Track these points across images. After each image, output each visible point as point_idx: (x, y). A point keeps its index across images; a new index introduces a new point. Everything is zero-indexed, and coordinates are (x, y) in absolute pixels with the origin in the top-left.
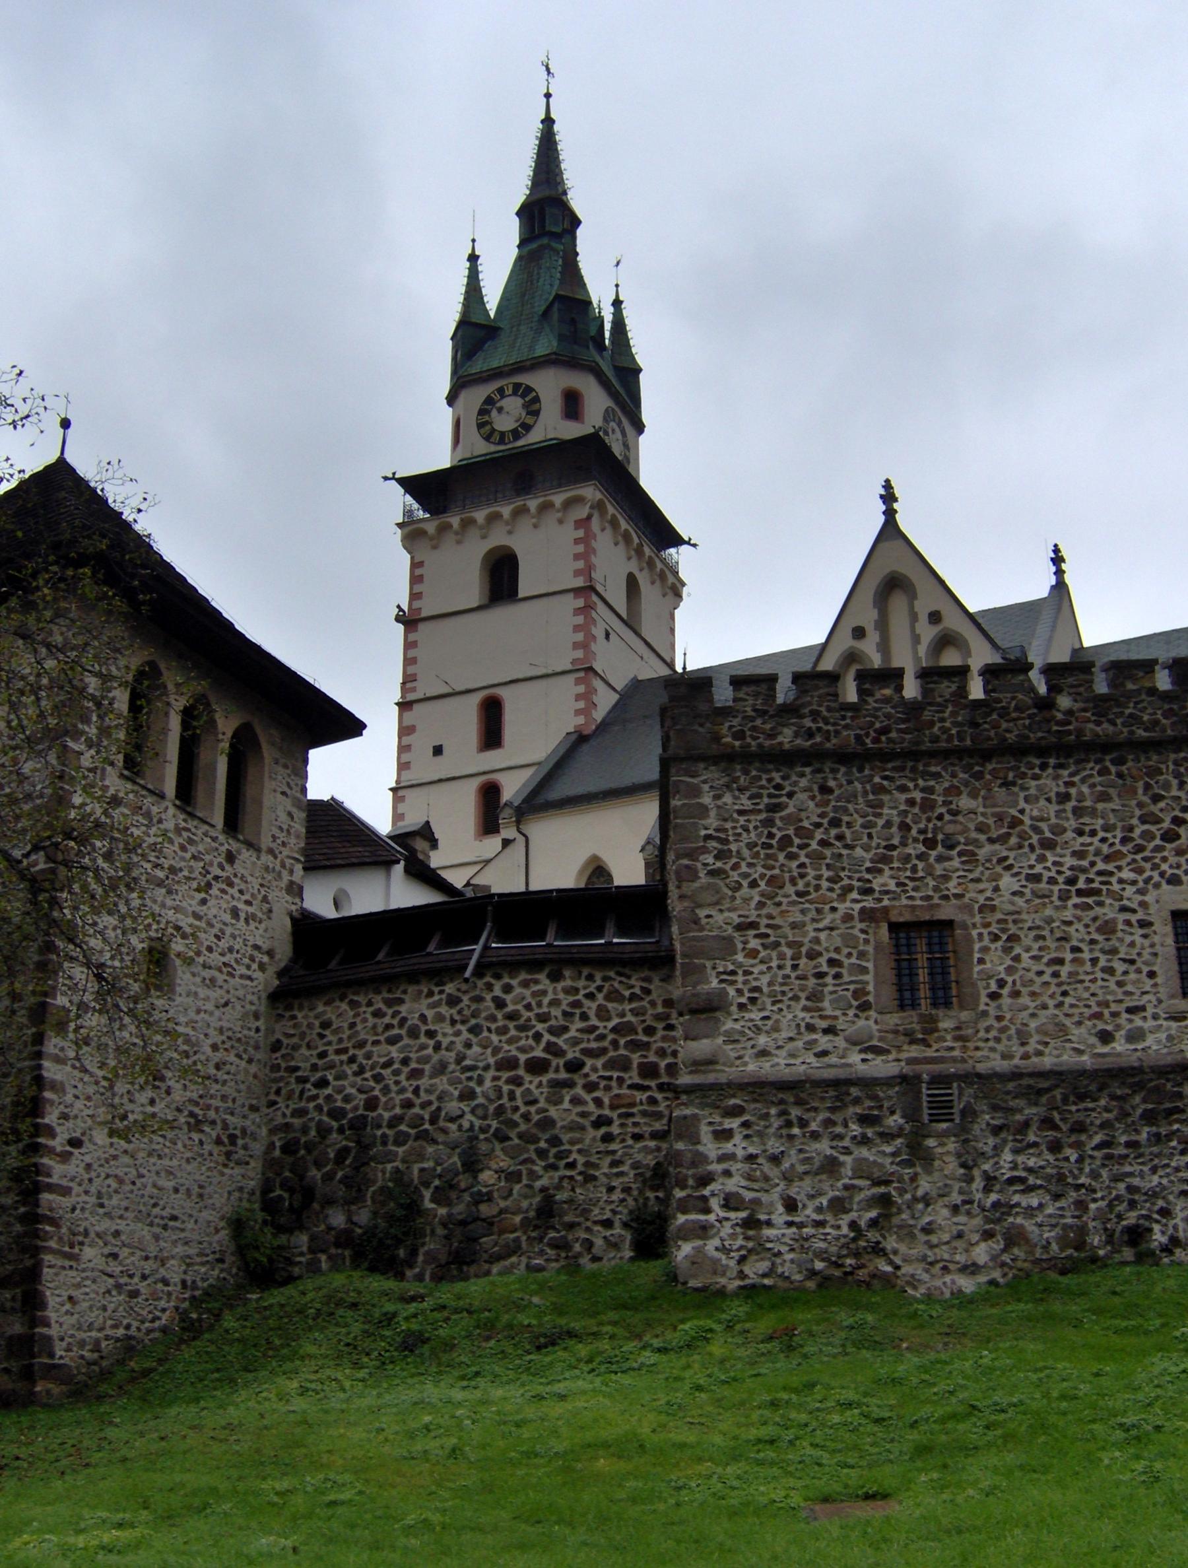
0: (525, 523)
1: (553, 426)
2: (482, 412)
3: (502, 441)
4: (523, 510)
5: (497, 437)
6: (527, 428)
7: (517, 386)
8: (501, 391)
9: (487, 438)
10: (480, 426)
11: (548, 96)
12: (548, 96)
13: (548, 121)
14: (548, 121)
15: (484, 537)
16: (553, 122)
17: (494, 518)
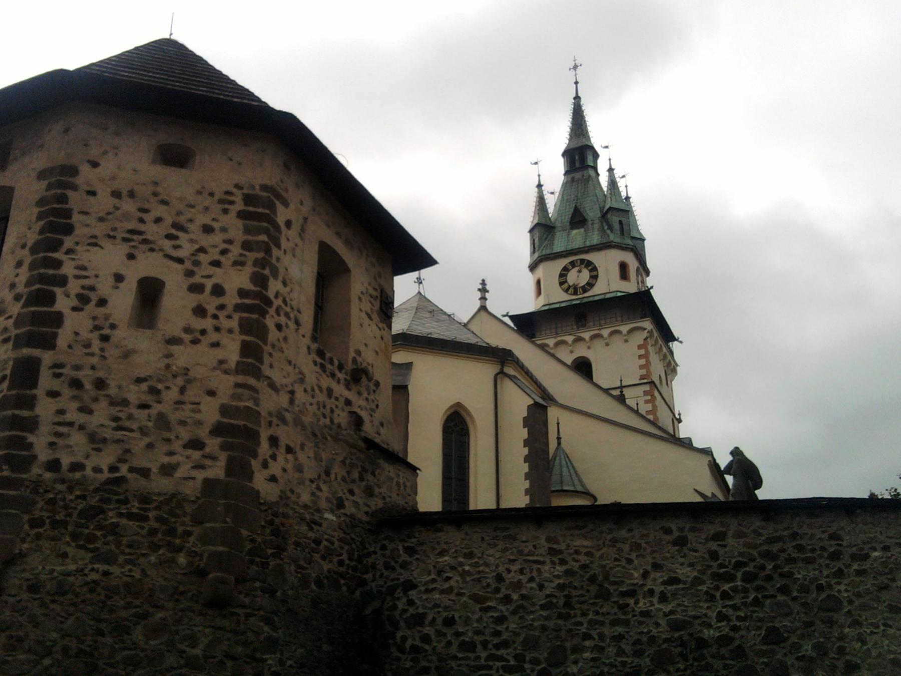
0: (598, 343)
1: (609, 284)
2: (561, 275)
3: (575, 293)
4: (598, 336)
5: (571, 290)
6: (590, 285)
7: (582, 261)
8: (573, 264)
9: (566, 291)
10: (561, 284)
11: (576, 83)
12: (576, 83)
13: (577, 98)
14: (577, 98)
15: (572, 352)
16: (580, 98)
17: (580, 339)
